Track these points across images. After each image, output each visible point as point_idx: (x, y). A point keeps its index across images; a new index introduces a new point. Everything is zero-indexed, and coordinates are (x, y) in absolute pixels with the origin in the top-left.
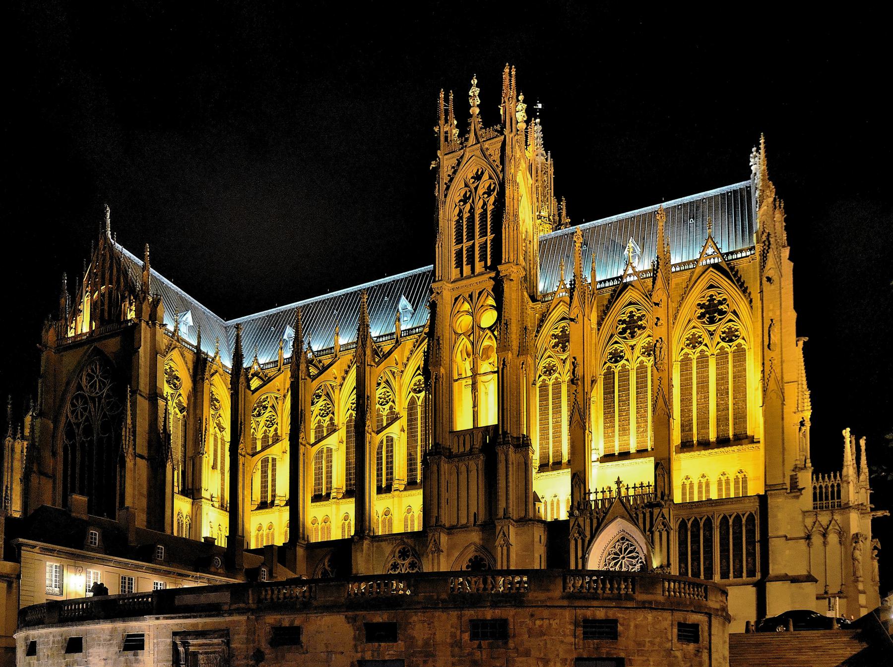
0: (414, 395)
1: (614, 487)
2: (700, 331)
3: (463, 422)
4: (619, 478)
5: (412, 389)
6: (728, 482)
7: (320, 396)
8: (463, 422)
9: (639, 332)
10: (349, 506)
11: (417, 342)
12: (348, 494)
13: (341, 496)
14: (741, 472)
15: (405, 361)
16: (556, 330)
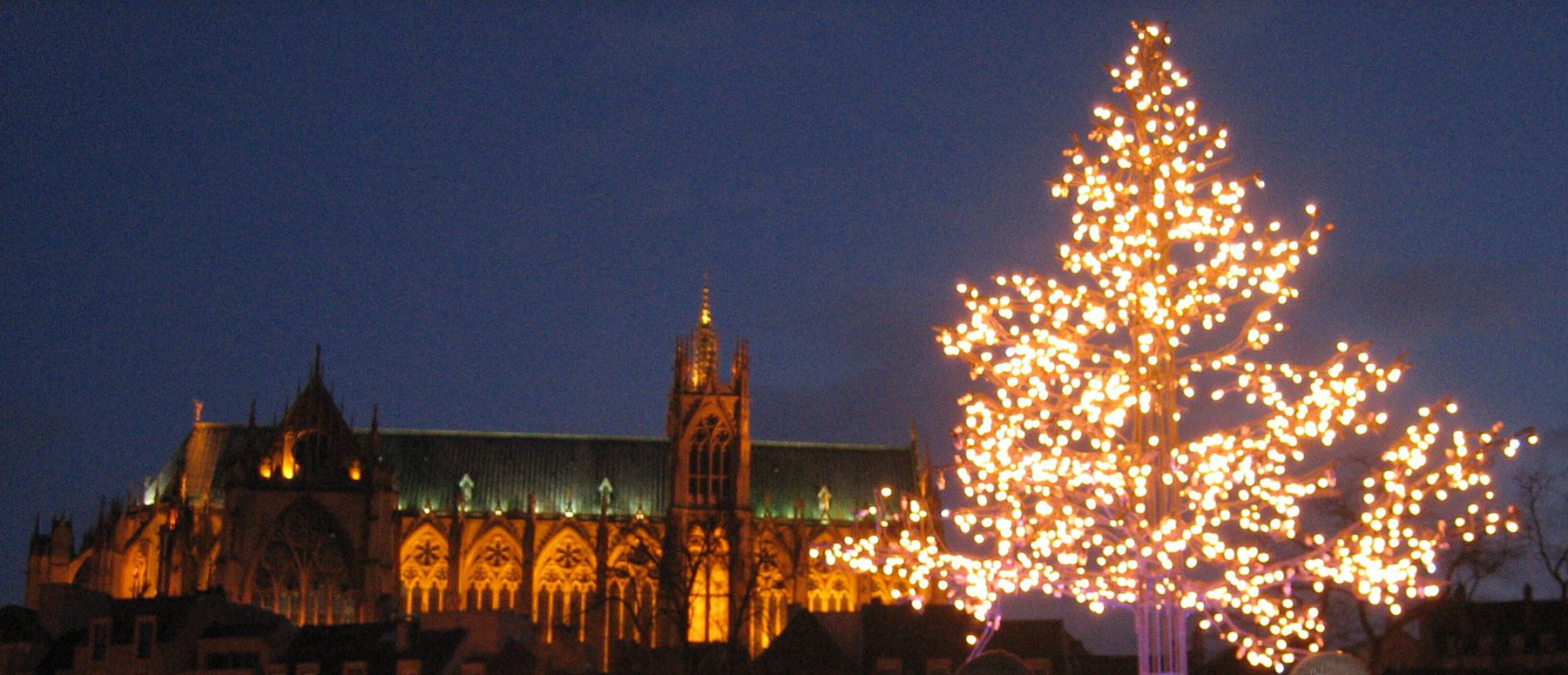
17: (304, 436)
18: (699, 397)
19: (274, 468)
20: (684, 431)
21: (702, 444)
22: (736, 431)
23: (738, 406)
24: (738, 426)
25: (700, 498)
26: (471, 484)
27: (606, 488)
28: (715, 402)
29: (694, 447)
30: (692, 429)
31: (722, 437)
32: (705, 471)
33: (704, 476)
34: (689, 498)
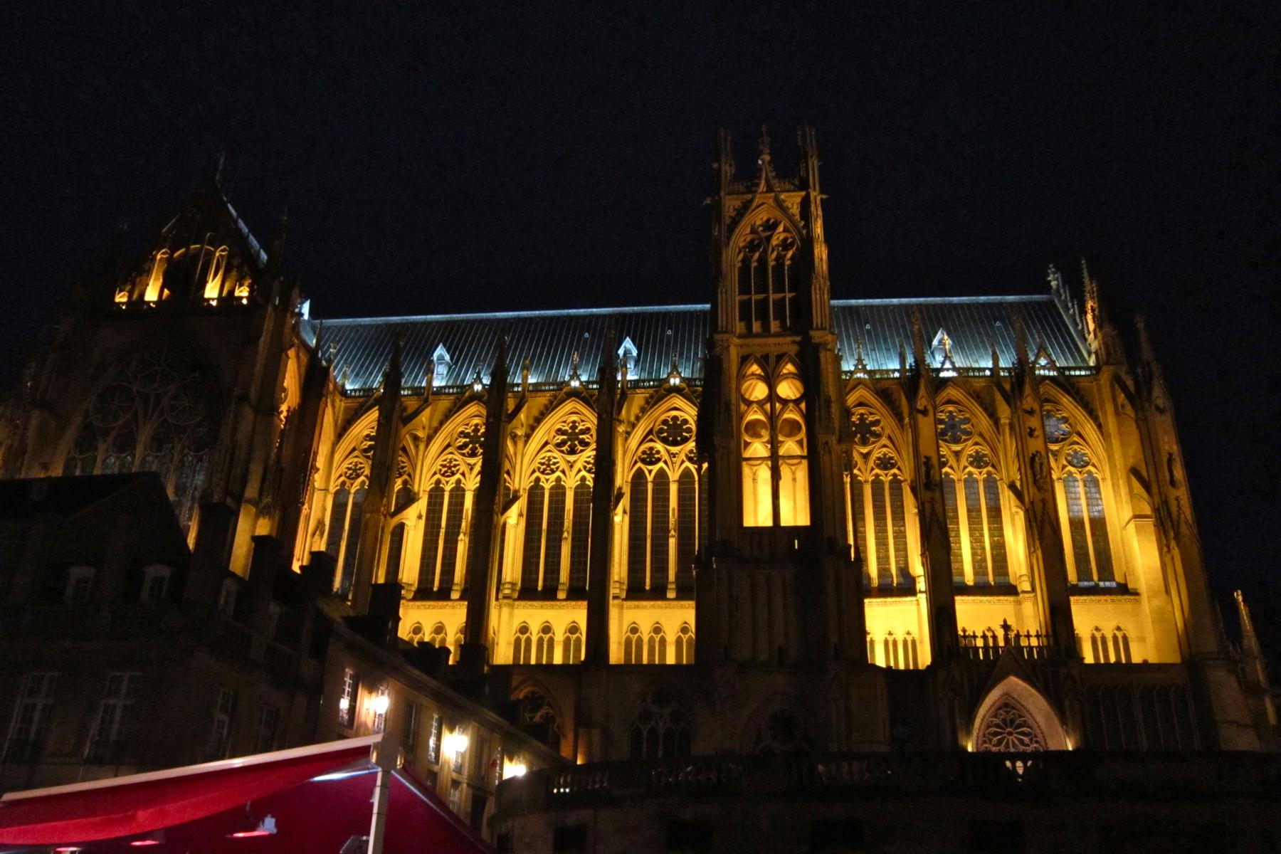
0: (643, 466)
1: (1000, 634)
2: (984, 448)
3: (757, 514)
4: (1005, 621)
5: (640, 458)
6: (895, 643)
7: (587, 444)
8: (757, 514)
9: (872, 439)
10: (578, 614)
11: (652, 397)
12: (575, 593)
13: (516, 595)
14: (1118, 629)
15: (633, 419)
16: (564, 424)
17: (183, 255)
18: (750, 196)
19: (135, 296)
20: (729, 238)
21: (757, 255)
22: (804, 232)
23: (805, 204)
24: (808, 225)
25: (756, 327)
26: (447, 357)
27: (627, 352)
28: (771, 201)
29: (746, 262)
30: (742, 236)
31: (785, 245)
32: (763, 289)
33: (761, 296)
34: (739, 327)
